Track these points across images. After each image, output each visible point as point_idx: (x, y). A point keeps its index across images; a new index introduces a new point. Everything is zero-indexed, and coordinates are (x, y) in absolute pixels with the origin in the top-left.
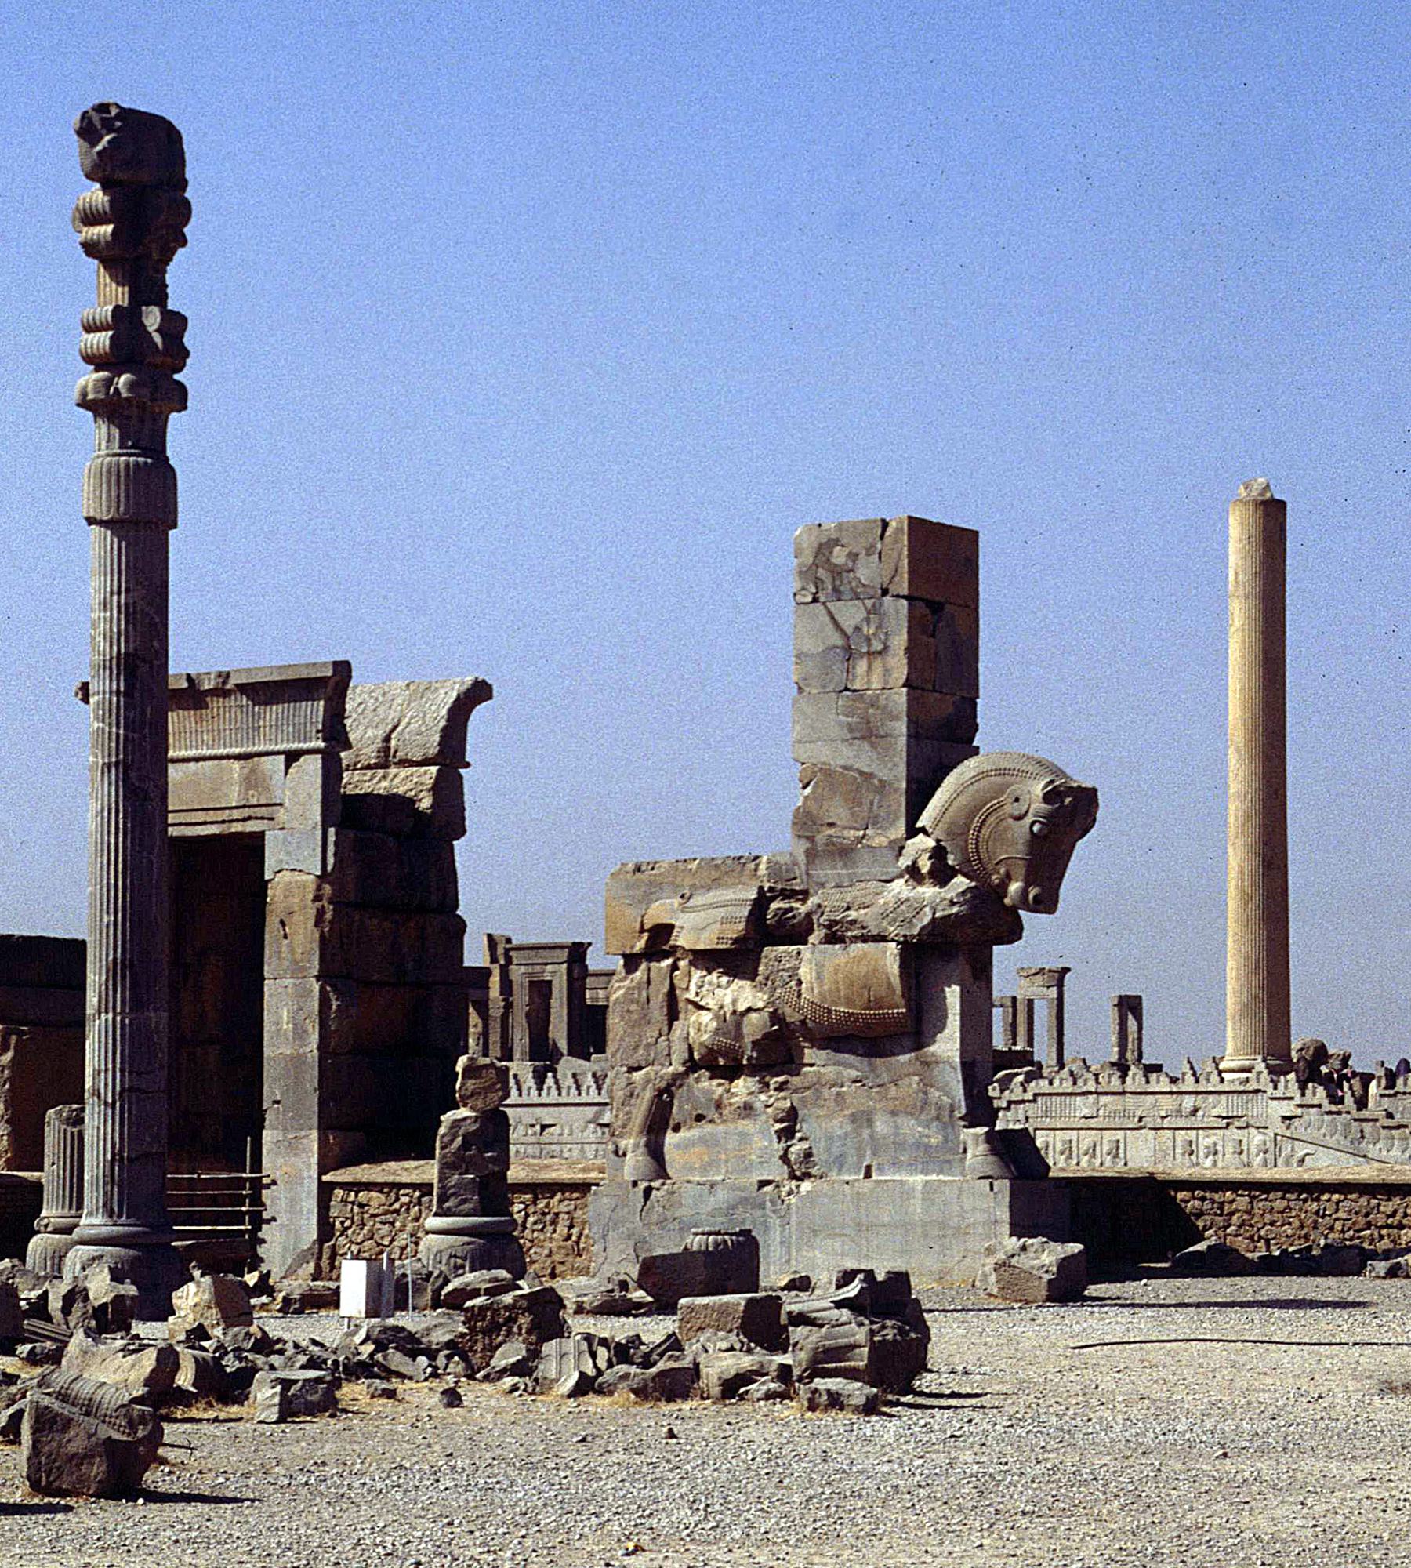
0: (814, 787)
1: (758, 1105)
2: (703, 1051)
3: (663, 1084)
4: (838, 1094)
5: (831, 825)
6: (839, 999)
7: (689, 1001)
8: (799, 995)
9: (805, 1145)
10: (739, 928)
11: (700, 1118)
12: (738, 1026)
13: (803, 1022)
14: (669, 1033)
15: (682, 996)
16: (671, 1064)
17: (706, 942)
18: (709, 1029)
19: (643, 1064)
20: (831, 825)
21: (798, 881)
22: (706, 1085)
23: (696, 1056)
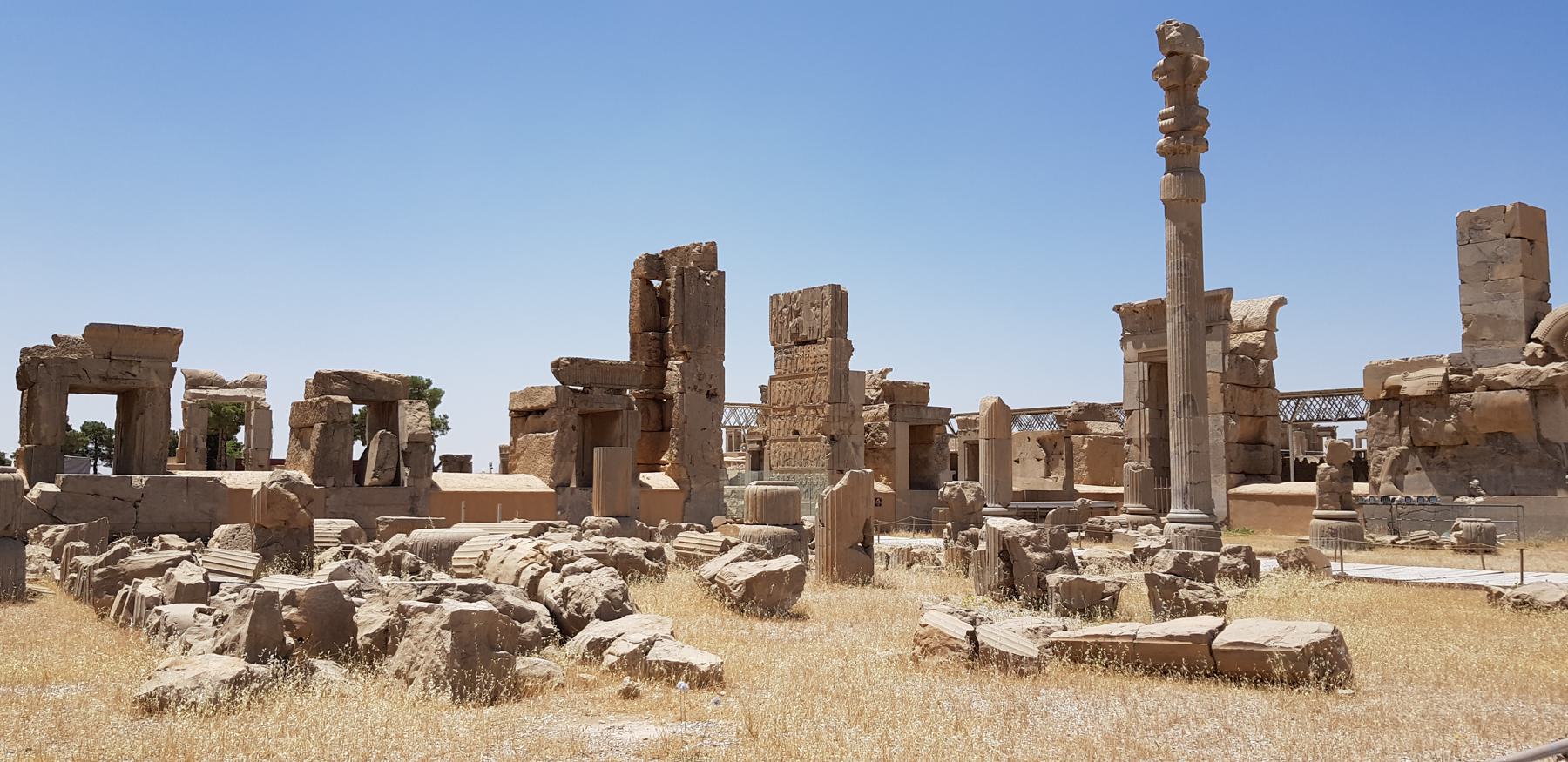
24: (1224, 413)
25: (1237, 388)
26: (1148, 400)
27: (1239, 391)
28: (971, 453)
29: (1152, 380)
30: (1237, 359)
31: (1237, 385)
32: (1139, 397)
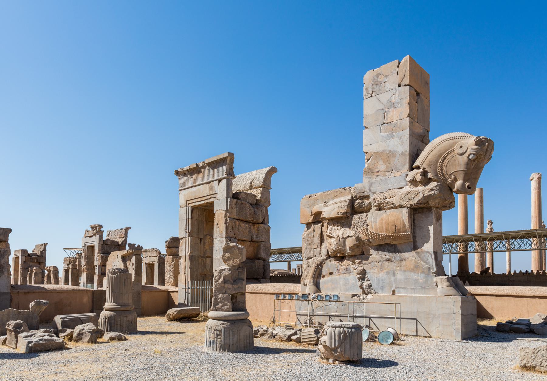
0: (371, 160)
1: (352, 269)
2: (332, 251)
3: (319, 263)
4: (381, 265)
5: (378, 171)
6: (383, 230)
7: (328, 236)
8: (367, 230)
9: (369, 282)
10: (344, 209)
11: (331, 273)
12: (344, 242)
13: (368, 240)
14: (321, 247)
15: (325, 234)
16: (321, 256)
17: (333, 215)
18: (334, 244)
19: (312, 257)
20: (378, 171)
21: (366, 192)
22: (332, 264)
23: (330, 253)
24: (225, 238)
25: (237, 222)
26: (190, 231)
27: (239, 224)
28: (149, 268)
29: (194, 220)
30: (237, 202)
31: (237, 219)
32: (186, 229)
